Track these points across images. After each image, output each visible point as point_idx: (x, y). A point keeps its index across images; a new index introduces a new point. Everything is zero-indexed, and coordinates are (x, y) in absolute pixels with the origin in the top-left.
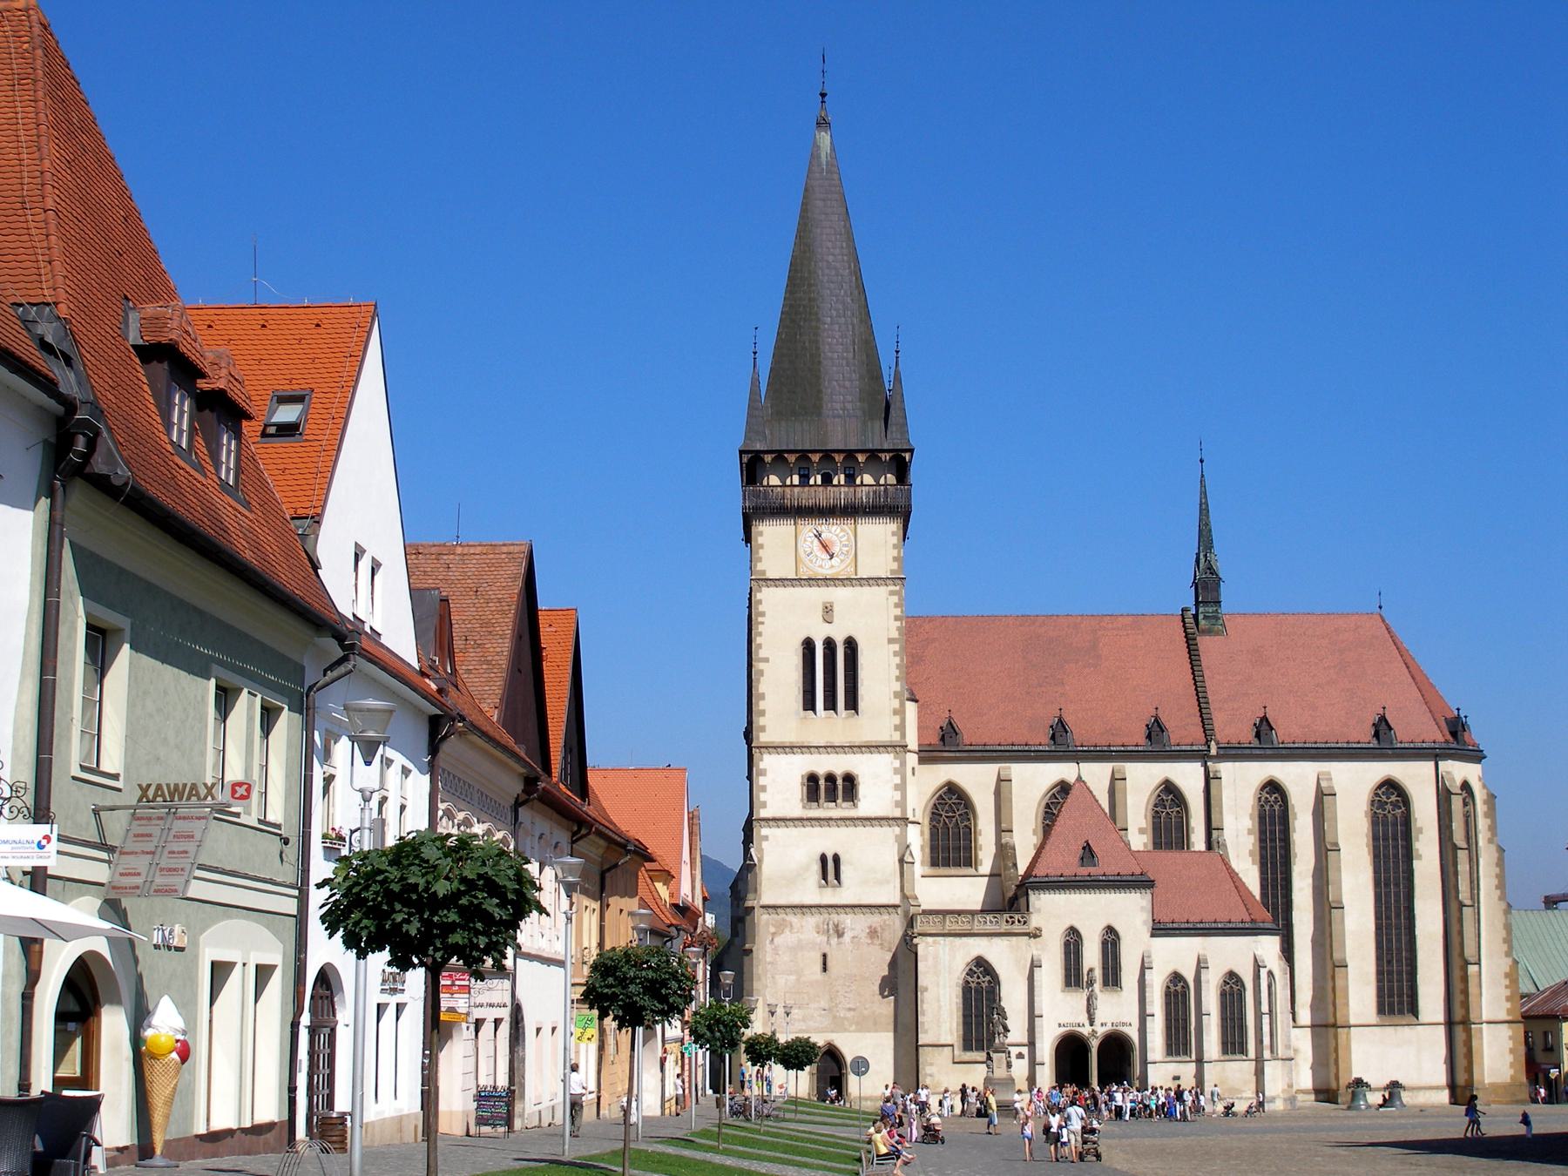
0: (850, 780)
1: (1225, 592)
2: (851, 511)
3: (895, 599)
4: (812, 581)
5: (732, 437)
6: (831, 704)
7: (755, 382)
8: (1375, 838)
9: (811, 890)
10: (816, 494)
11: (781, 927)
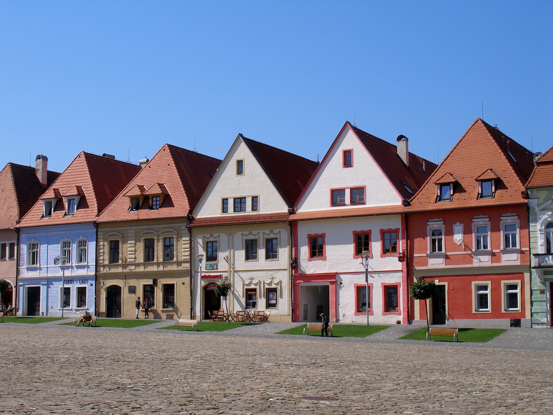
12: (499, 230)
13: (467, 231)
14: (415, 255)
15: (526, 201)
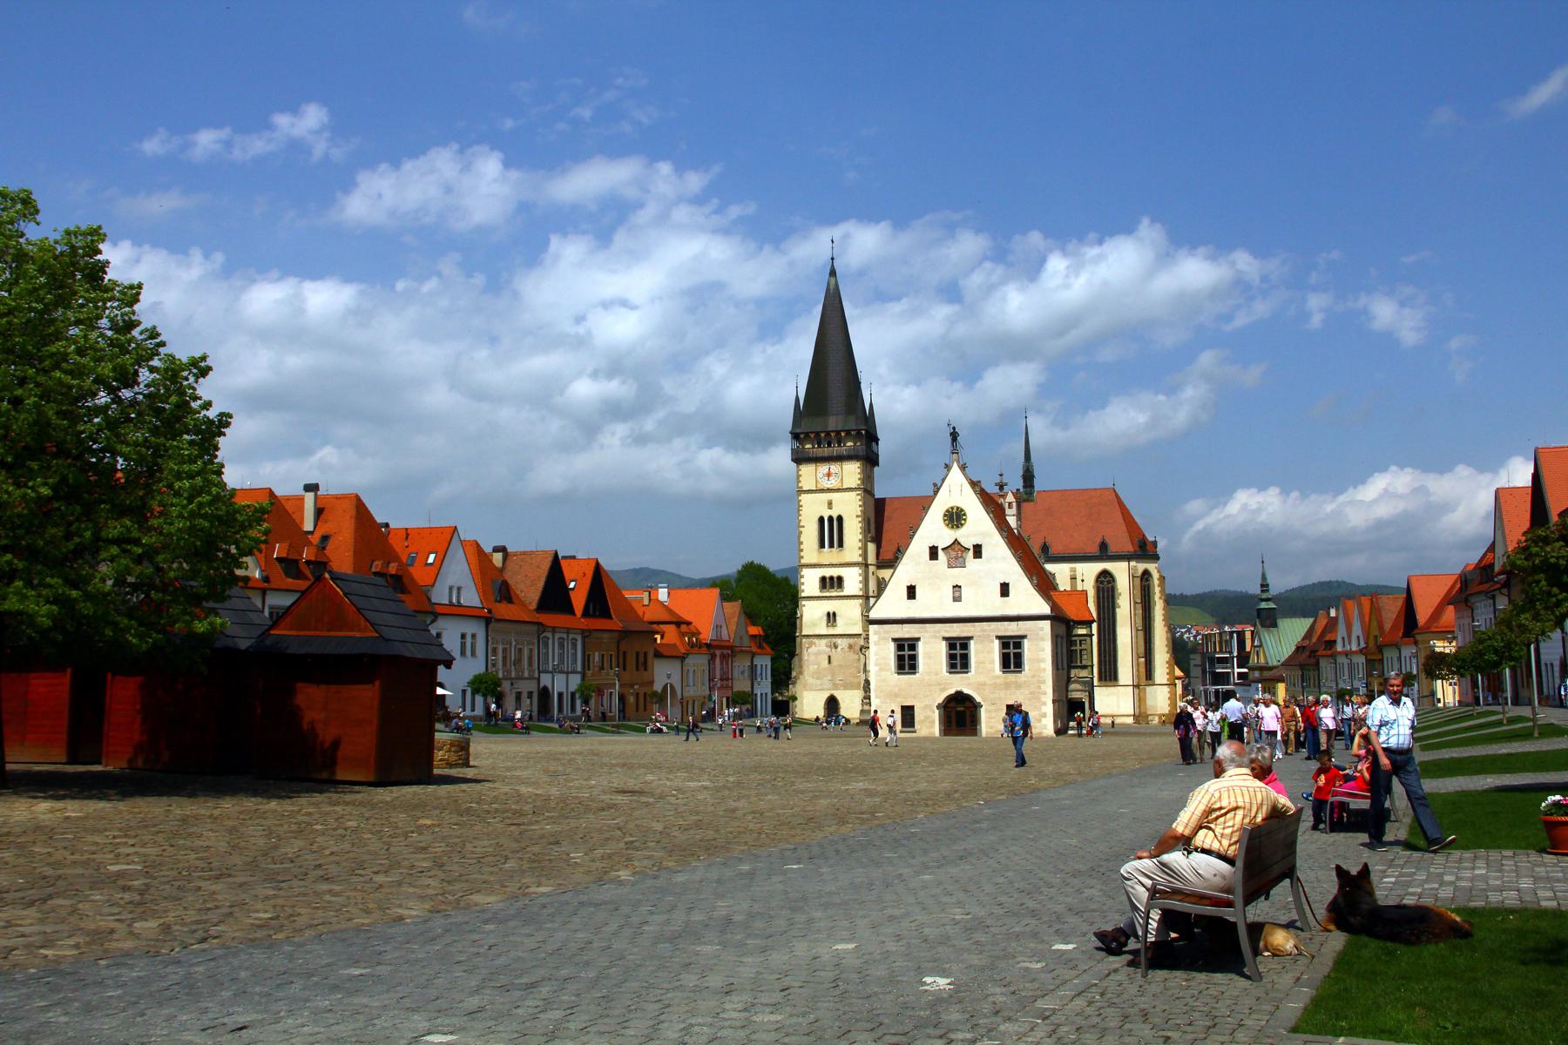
0: (840, 579)
2: (840, 458)
7: (797, 399)
9: (823, 629)
10: (826, 451)
11: (811, 644)
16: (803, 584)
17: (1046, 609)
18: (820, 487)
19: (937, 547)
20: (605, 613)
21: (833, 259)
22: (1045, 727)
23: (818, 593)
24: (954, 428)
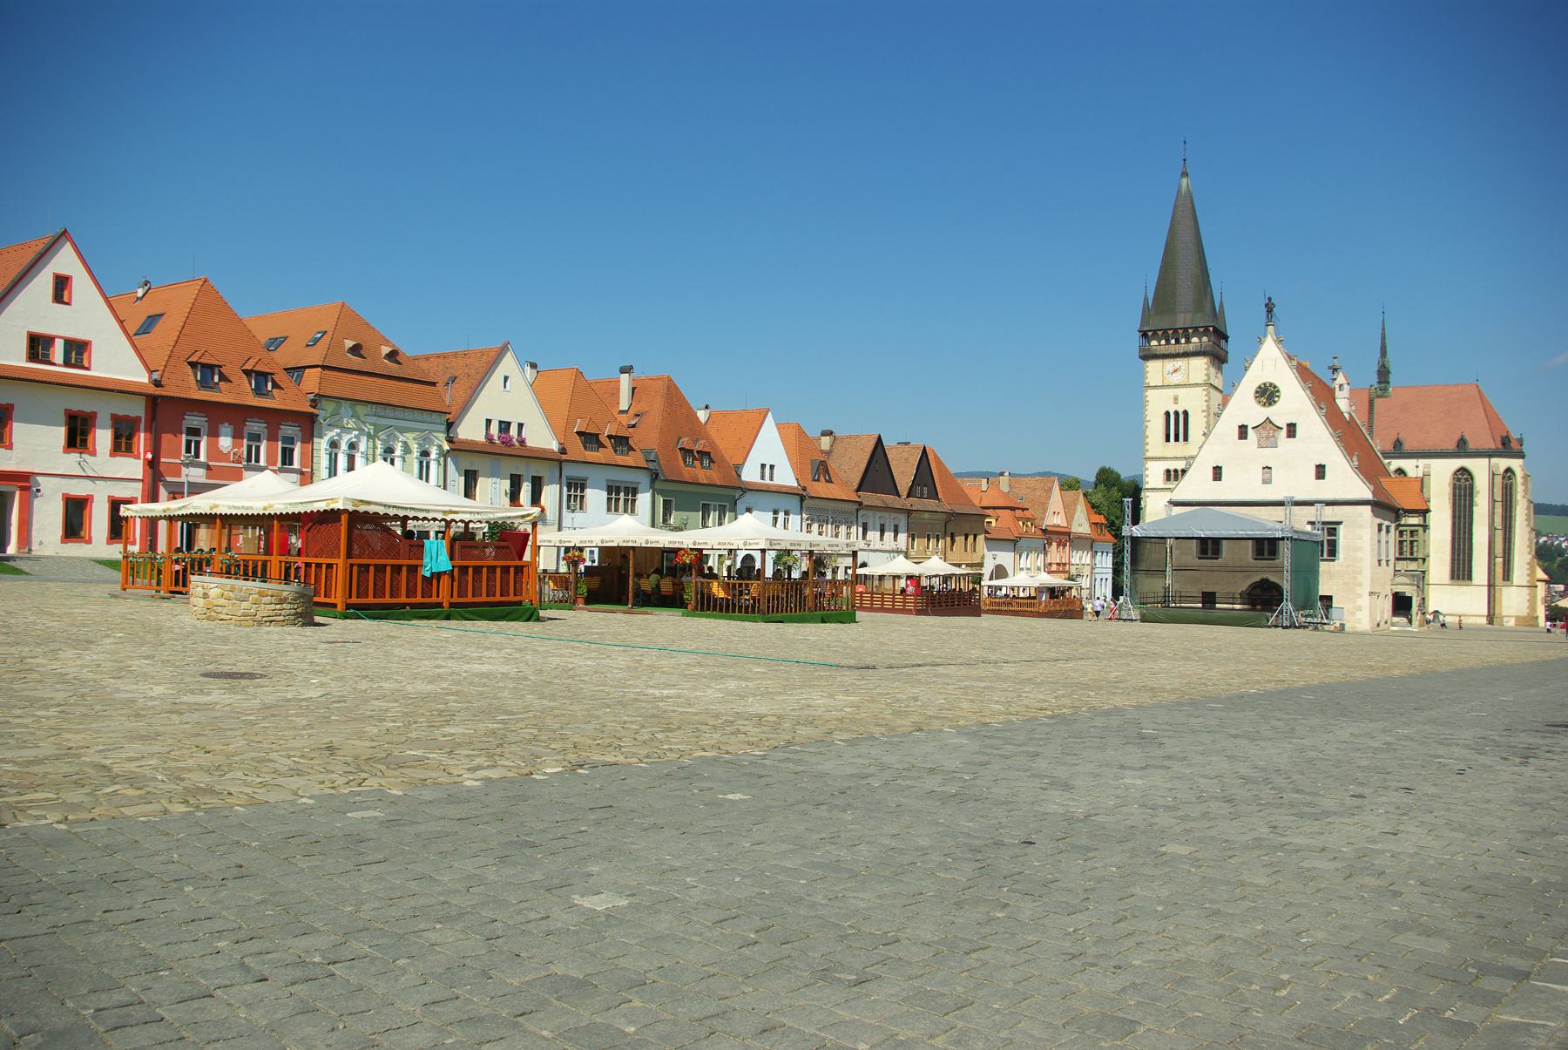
1: (1392, 378)
2: (1186, 355)
3: (1205, 393)
4: (1169, 386)
5: (1135, 322)
6: (1177, 439)
7: (1146, 299)
8: (1454, 495)
10: (1173, 347)
12: (243, 438)
13: (237, 436)
14: (162, 460)
15: (312, 410)
16: (1147, 476)
17: (1368, 495)
18: (1166, 383)
19: (1247, 426)
20: (934, 495)
21: (1185, 160)
22: (1359, 621)
23: (1162, 486)
24: (1270, 299)
